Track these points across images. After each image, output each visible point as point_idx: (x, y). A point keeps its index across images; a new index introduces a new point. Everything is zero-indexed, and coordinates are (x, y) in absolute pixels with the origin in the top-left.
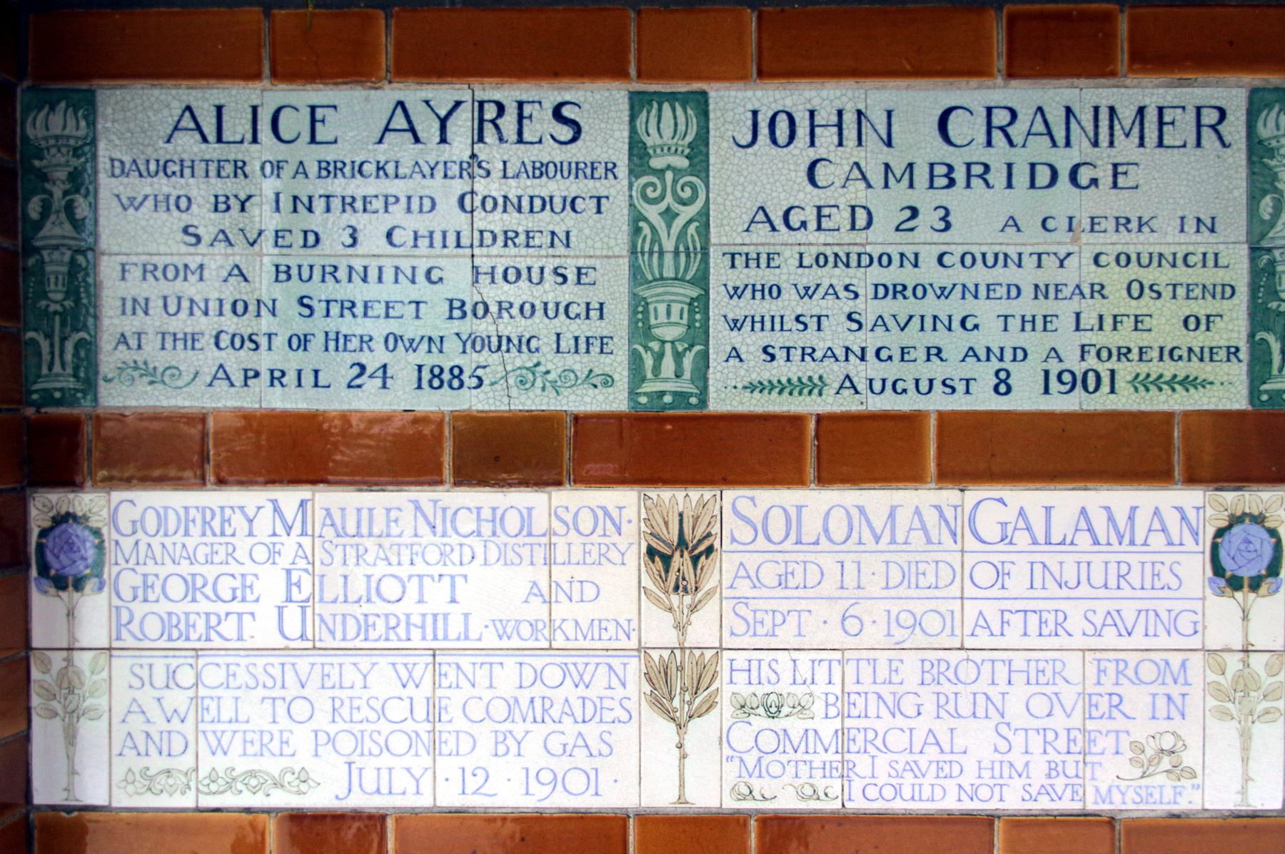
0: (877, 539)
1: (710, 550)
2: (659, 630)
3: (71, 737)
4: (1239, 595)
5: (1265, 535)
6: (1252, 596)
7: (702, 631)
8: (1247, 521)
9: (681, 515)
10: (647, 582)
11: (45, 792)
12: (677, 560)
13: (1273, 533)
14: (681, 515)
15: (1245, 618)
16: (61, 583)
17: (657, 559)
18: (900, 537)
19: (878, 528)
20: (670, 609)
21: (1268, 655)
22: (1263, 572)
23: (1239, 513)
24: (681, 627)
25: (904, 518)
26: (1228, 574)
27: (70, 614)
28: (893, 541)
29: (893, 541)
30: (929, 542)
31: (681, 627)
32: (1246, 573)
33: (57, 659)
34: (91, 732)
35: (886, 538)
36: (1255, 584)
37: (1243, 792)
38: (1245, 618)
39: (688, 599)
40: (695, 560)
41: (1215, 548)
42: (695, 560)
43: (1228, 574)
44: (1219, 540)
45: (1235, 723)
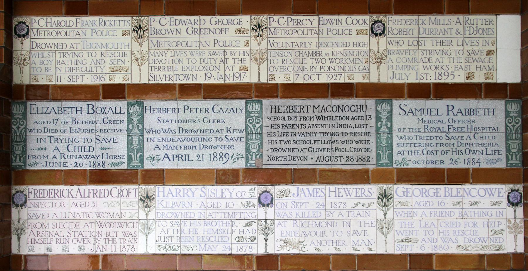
1: (154, 198)
2: (142, 215)
3: (19, 239)
7: (152, 216)
11: (14, 251)
12: (147, 200)
13: (271, 195)
15: (266, 213)
16: (17, 206)
24: (147, 215)
27: (19, 211)
32: (266, 203)
33: (16, 222)
34: (23, 238)
36: (268, 205)
38: (266, 213)
40: (150, 200)
41: (259, 197)
42: (150, 200)
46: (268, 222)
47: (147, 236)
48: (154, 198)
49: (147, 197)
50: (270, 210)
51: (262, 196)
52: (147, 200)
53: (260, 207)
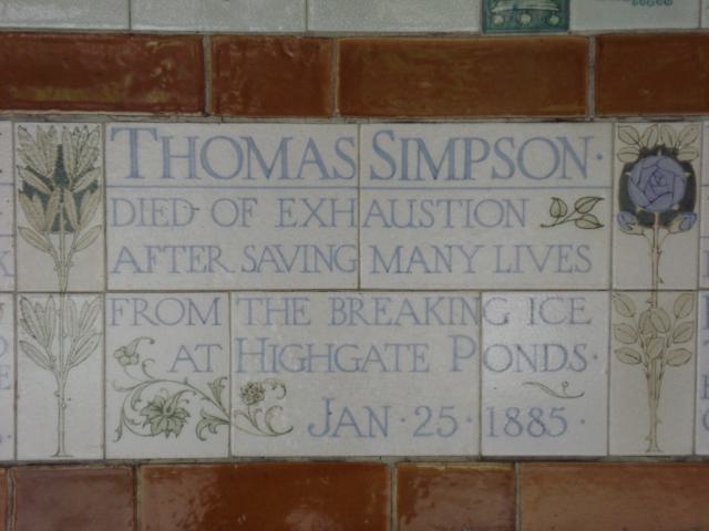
0: (268, 173)
2: (39, 270)
4: (648, 232)
5: (679, 170)
6: (663, 232)
7: (85, 273)
8: (659, 153)
9: (60, 148)
10: (22, 219)
12: (56, 191)
13: (687, 166)
14: (60, 148)
17: (35, 197)
18: (292, 173)
19: (268, 162)
20: (49, 249)
21: (679, 294)
22: (676, 208)
23: (650, 146)
24: (63, 266)
25: (296, 151)
26: (639, 209)
28: (284, 176)
29: (284, 176)
30: (326, 176)
31: (63, 266)
35: (277, 172)
36: (666, 220)
37: (651, 439)
39: (70, 237)
40: (79, 198)
41: (624, 181)
43: (639, 209)
44: (629, 174)
45: (641, 366)
46: (664, 300)
47: (61, 375)
48: (93, 187)
49: (61, 177)
50: (678, 245)
51: (634, 175)
52: (56, 191)
53: (628, 228)
